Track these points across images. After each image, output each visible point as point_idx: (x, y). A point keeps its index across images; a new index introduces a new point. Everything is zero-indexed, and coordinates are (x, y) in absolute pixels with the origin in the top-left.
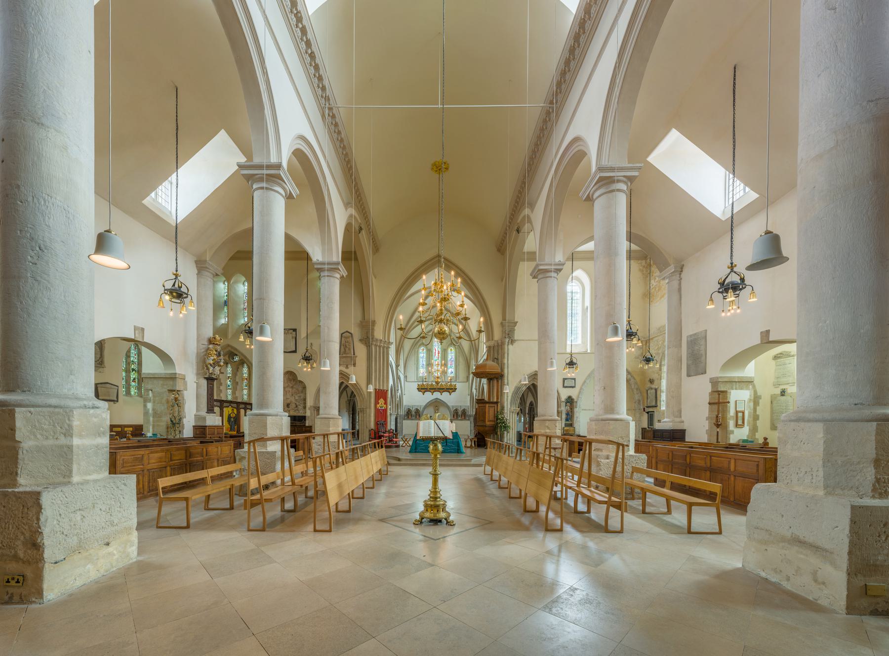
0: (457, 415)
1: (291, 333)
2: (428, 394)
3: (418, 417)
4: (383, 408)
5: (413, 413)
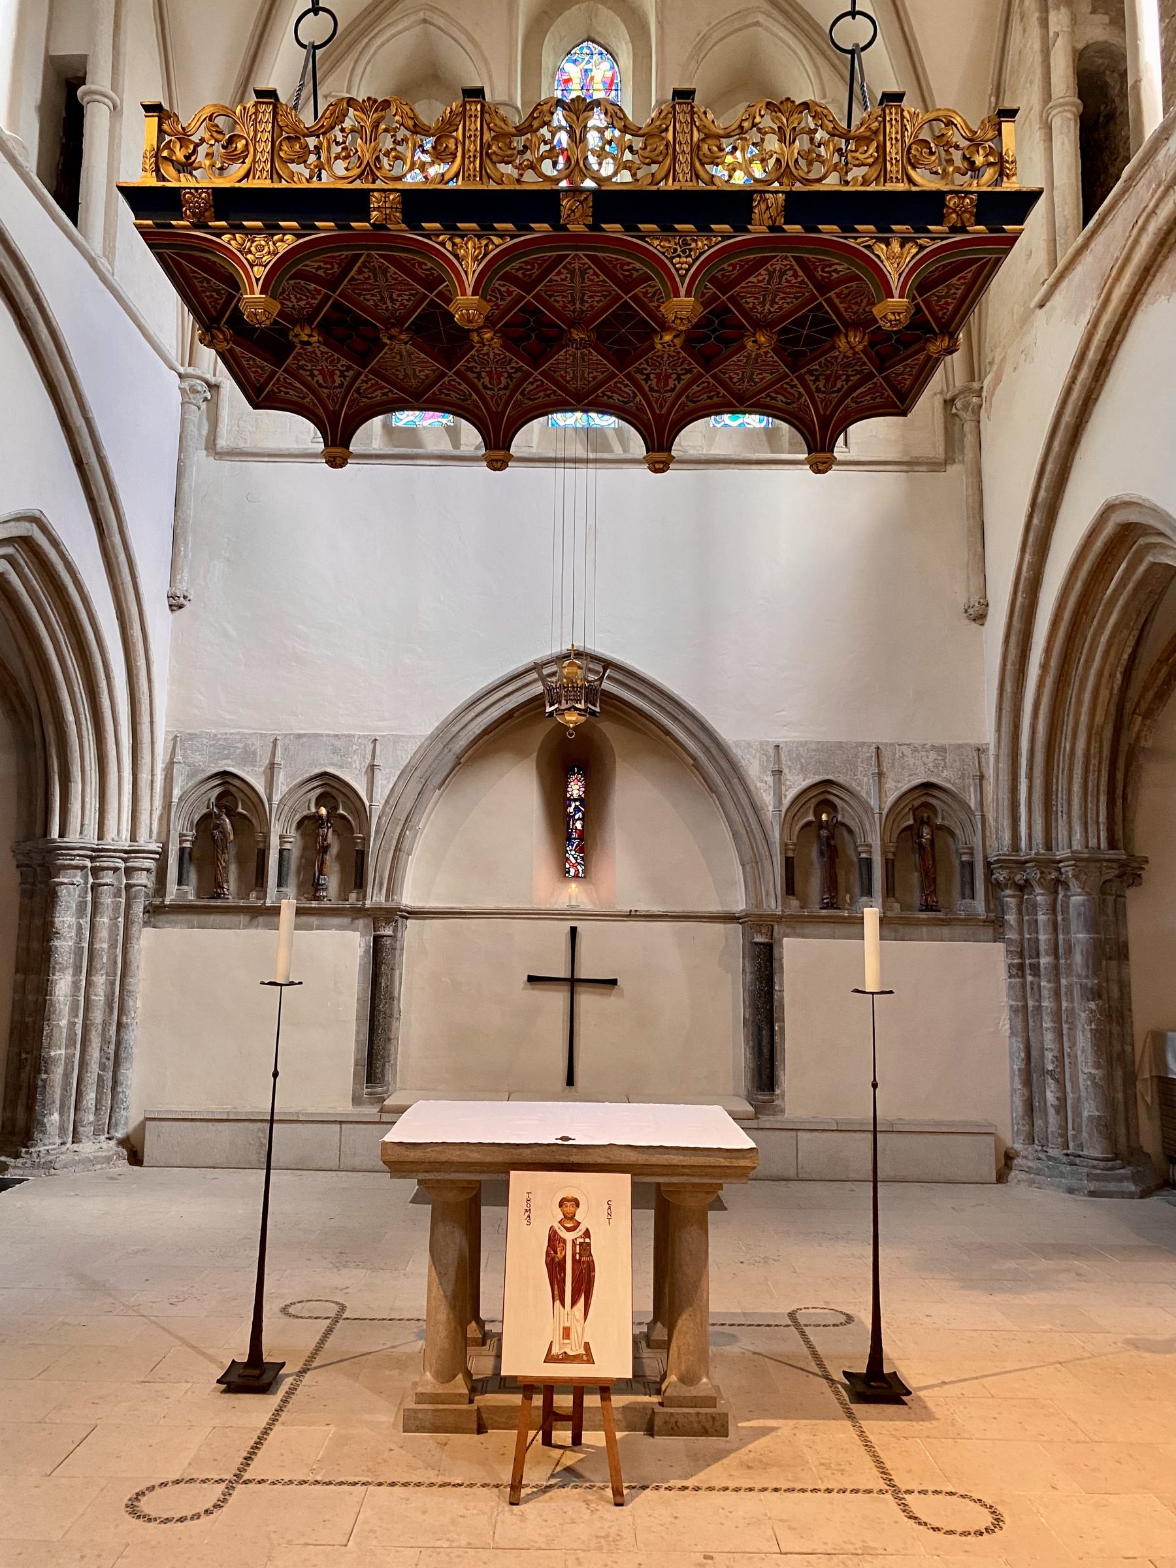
0: (831, 852)
3: (332, 881)
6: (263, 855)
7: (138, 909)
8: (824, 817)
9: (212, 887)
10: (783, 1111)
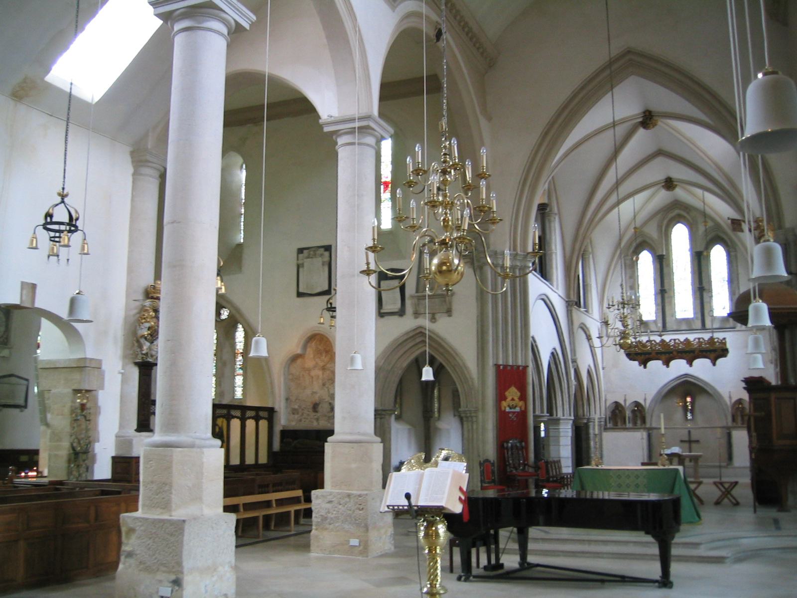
1: (322, 255)
2: (655, 365)
3: (639, 422)
4: (518, 409)
5: (628, 414)
7: (603, 428)
9: (616, 424)
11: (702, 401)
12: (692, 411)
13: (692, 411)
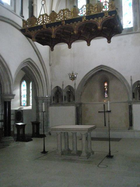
3: (71, 100)
5: (64, 94)
6: (62, 96)
8: (139, 86)
10: (133, 129)
11: (113, 84)
12: (108, 92)
13: (108, 92)
